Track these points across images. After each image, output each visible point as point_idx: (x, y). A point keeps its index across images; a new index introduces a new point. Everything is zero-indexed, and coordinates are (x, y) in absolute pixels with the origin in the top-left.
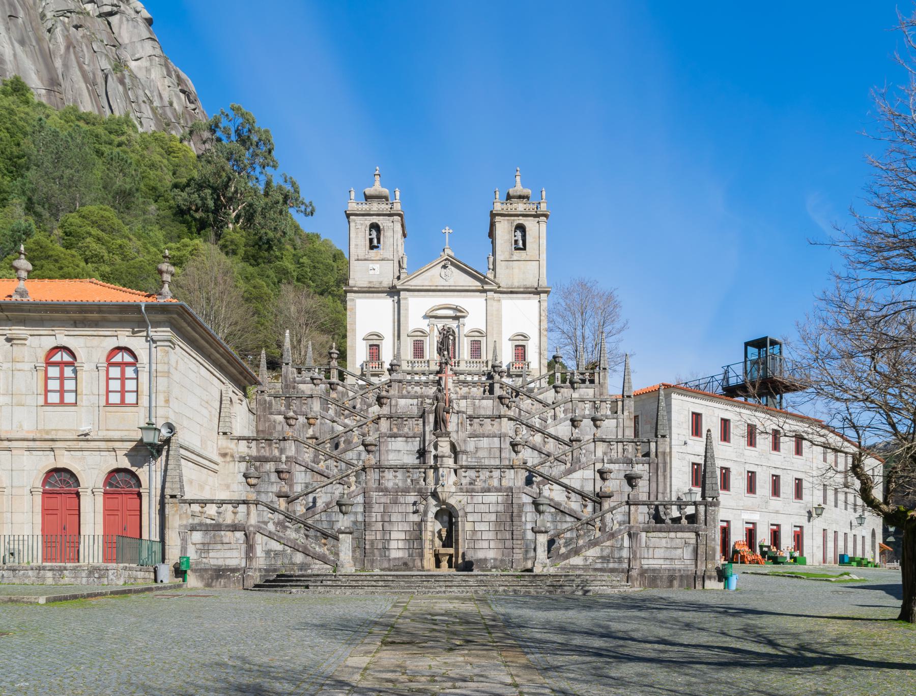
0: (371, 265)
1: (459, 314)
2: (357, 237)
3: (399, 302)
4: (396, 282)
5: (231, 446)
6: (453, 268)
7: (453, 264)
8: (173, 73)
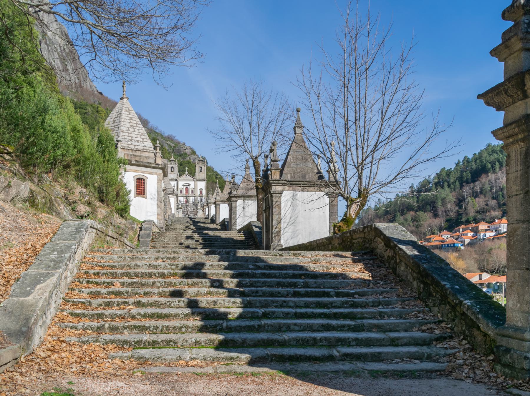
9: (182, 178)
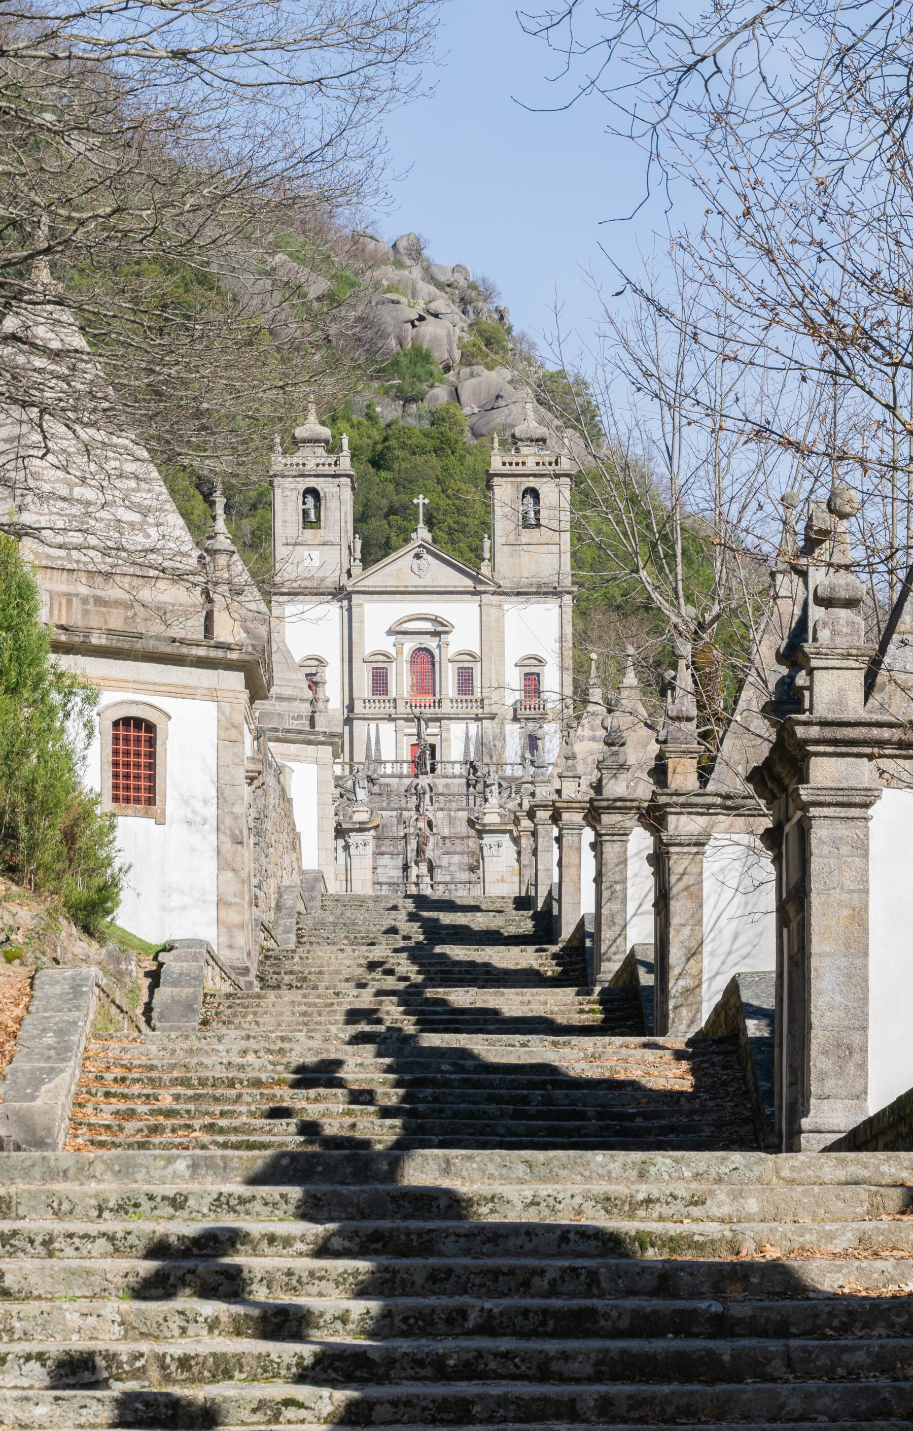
1: (440, 629)
2: (285, 509)
3: (350, 610)
4: (344, 580)
6: (430, 558)
7: (429, 552)
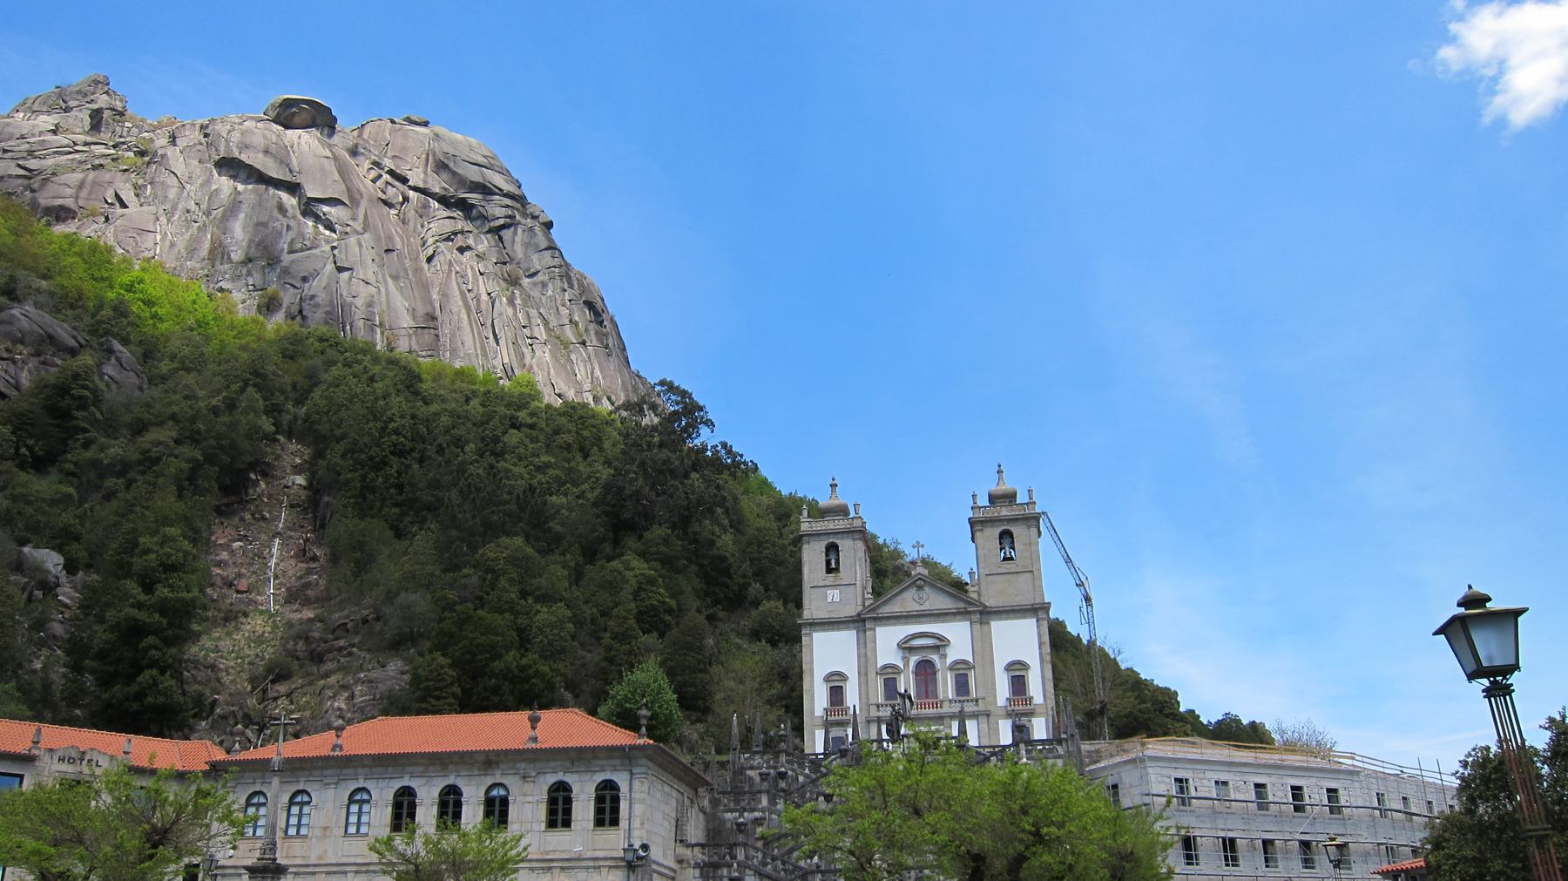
0: (830, 592)
1: (938, 643)
5: (688, 852)
8: (575, 283)
9: (887, 610)
